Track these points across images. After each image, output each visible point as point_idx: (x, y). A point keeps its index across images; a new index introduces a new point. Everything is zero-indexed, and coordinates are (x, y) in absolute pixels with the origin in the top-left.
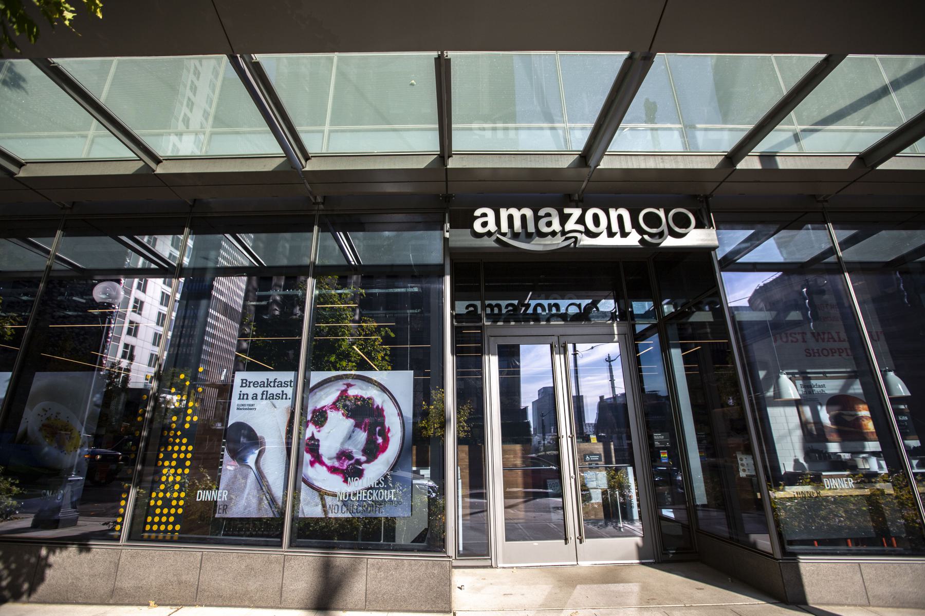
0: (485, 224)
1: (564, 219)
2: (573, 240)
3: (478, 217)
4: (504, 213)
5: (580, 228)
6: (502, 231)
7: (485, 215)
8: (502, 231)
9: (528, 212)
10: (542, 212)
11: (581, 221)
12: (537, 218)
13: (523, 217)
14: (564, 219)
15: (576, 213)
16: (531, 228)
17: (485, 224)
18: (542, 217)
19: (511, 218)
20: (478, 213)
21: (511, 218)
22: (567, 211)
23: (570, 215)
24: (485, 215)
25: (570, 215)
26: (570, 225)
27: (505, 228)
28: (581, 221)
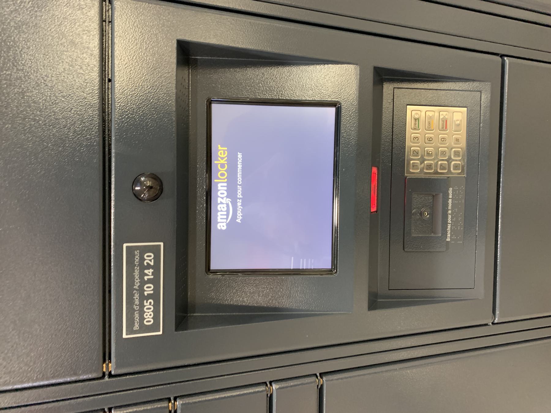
1: (221, 203)
2: (229, 201)
4: (219, 220)
5: (225, 198)
6: (226, 221)
7: (220, 226)
8: (226, 221)
10: (219, 209)
11: (222, 198)
12: (221, 211)
13: (221, 215)
14: (221, 203)
15: (219, 200)
17: (223, 226)
19: (221, 219)
20: (219, 228)
21: (221, 219)
22: (219, 202)
23: (221, 202)
25: (221, 202)
26: (224, 201)
27: (225, 220)
28: (222, 198)
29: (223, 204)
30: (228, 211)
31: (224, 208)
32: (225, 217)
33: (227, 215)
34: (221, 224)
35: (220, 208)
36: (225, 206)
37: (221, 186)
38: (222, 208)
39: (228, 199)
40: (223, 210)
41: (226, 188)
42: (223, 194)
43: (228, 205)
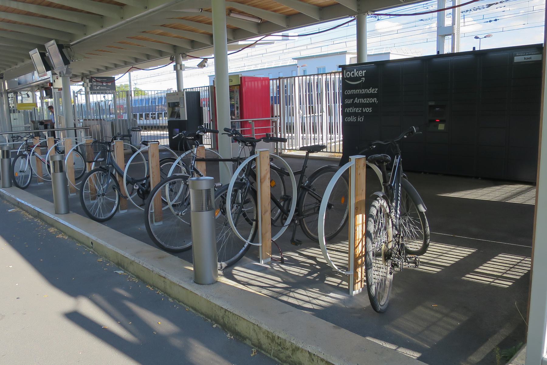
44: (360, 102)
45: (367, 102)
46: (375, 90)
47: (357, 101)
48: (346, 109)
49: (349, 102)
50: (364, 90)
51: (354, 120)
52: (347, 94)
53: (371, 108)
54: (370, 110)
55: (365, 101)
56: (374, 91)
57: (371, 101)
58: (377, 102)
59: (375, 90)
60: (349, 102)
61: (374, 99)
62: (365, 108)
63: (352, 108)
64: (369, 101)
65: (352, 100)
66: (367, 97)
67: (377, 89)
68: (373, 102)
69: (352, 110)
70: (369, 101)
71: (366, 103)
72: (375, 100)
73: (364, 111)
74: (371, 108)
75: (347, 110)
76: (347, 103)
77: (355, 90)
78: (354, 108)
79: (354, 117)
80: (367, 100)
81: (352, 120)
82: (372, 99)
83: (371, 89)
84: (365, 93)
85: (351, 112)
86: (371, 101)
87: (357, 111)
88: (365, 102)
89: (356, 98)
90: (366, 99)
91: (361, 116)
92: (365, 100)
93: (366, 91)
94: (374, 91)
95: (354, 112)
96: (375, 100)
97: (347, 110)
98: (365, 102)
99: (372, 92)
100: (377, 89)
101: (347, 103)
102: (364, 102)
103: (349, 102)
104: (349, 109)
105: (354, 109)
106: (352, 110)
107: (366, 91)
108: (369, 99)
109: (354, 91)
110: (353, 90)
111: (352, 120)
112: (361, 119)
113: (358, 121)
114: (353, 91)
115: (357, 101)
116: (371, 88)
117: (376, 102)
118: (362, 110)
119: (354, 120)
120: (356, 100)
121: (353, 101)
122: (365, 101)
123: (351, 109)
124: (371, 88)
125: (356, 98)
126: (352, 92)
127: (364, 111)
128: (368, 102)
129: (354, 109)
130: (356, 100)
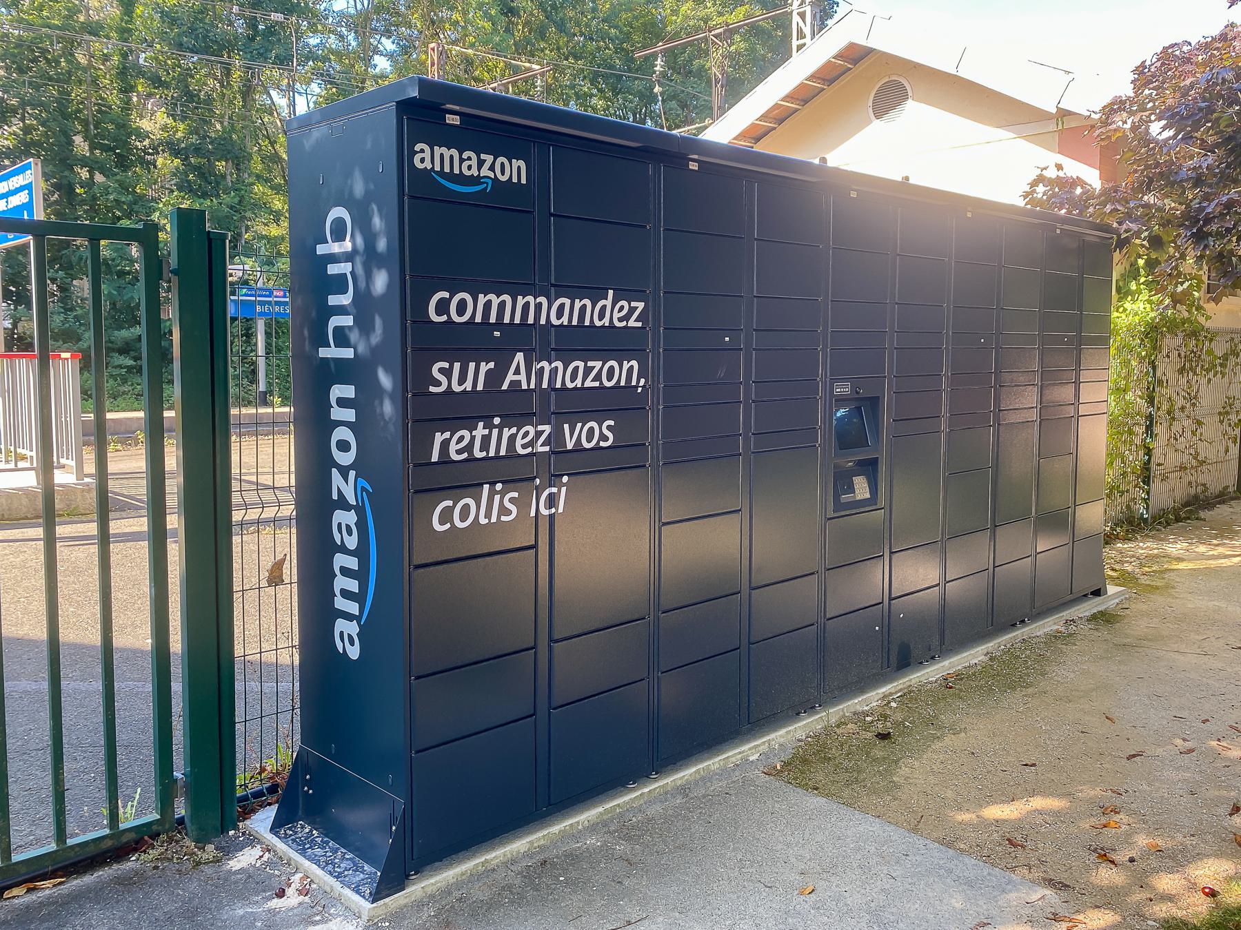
0: (422, 160)
1: (481, 163)
3: (417, 152)
4: (438, 150)
7: (422, 151)
9: (454, 152)
10: (465, 156)
11: (492, 168)
12: (462, 161)
14: (481, 163)
15: (489, 159)
16: (456, 171)
17: (422, 160)
18: (465, 160)
19: (442, 155)
20: (418, 147)
21: (442, 155)
22: (483, 156)
24: (422, 151)
27: (437, 168)
28: (492, 168)
29: (479, 170)
30: (461, 179)
31: (470, 168)
32: (447, 170)
33: (451, 177)
34: (427, 155)
35: (469, 159)
36: (474, 172)
37: (519, 167)
38: (468, 163)
39: (490, 182)
40: (465, 164)
41: (515, 180)
42: (503, 173)
43: (476, 180)
44: (545, 385)
45: (588, 384)
46: (632, 310)
47: (518, 373)
48: (439, 438)
49: (468, 386)
50: (567, 302)
51: (504, 511)
52: (450, 322)
53: (612, 423)
54: (603, 437)
55: (574, 377)
56: (626, 318)
57: (610, 378)
58: (642, 381)
59: (632, 310)
60: (462, 380)
61: (626, 365)
62: (579, 425)
63: (488, 426)
64: (598, 377)
65: (484, 367)
66: (587, 353)
67: (641, 305)
68: (623, 383)
69: (486, 440)
70: (598, 377)
71: (583, 388)
72: (631, 369)
73: (570, 446)
74: (612, 423)
75: (445, 444)
76: (449, 390)
77: (506, 298)
78: (501, 428)
79: (503, 493)
80: (588, 371)
81: (488, 515)
82: (613, 363)
83: (608, 303)
84: (575, 322)
85: (478, 454)
86: (610, 378)
87: (524, 446)
88: (578, 383)
89: (520, 357)
90: (581, 364)
91: (553, 480)
92: (576, 369)
93: (583, 309)
94: (626, 318)
95: (503, 452)
96: (631, 369)
97: (445, 444)
98: (578, 383)
99: (617, 324)
100: (641, 305)
101: (449, 390)
102: (570, 385)
103: (462, 380)
104: (465, 433)
105: (507, 433)
106: (486, 440)
107: (583, 309)
108: (598, 364)
109: (502, 305)
110: (492, 296)
111: (488, 515)
112: (552, 501)
113: (533, 514)
114: (496, 301)
115: (522, 377)
116: (611, 292)
117: (638, 381)
118: (556, 438)
119: (504, 511)
120: (517, 372)
121: (495, 378)
122: (574, 377)
123: (480, 431)
124: (611, 292)
125: (520, 357)
126: (488, 305)
127: (570, 446)
128: (597, 384)
129: (507, 433)
130: (517, 372)
